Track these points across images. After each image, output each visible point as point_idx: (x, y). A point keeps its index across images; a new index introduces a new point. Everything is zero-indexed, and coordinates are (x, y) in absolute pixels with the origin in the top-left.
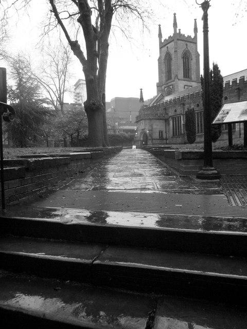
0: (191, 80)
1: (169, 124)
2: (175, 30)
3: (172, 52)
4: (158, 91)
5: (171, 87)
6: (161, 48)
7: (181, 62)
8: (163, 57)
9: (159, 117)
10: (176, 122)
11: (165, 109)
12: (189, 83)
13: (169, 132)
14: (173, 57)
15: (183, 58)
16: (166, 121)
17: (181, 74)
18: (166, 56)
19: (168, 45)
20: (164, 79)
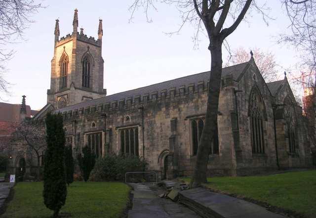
5: (66, 96)
12: (88, 94)
19: (65, 45)
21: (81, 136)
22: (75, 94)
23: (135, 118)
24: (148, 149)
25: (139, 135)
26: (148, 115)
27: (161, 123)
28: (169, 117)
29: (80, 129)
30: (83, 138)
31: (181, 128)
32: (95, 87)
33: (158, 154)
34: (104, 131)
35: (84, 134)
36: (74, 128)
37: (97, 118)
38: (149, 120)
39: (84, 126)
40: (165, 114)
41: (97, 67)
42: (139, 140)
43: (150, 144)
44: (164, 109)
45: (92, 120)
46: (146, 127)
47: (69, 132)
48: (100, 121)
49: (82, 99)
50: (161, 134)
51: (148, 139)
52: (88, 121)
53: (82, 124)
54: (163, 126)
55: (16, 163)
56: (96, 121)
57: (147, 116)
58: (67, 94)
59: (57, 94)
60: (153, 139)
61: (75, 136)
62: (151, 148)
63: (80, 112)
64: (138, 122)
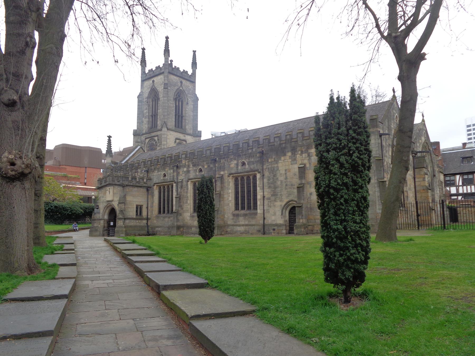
0: (185, 133)
1: (153, 196)
4: (135, 142)
9: (139, 182)
10: (164, 192)
11: (147, 172)
12: (181, 136)
13: (152, 207)
15: (175, 99)
16: (148, 190)
20: (145, 127)
21: (184, 183)
22: (167, 135)
23: (253, 164)
25: (258, 183)
26: (270, 161)
27: (286, 170)
28: (296, 163)
29: (183, 175)
30: (187, 185)
35: (188, 181)
36: (175, 174)
37: (205, 163)
38: (270, 166)
40: (290, 160)
42: (258, 188)
44: (289, 154)
45: (198, 165)
46: (267, 174)
47: (169, 179)
48: (209, 166)
49: (175, 142)
51: (269, 187)
53: (185, 169)
55: (104, 215)
57: (268, 161)
60: (275, 188)
61: (177, 183)
63: (184, 156)
64: (256, 168)
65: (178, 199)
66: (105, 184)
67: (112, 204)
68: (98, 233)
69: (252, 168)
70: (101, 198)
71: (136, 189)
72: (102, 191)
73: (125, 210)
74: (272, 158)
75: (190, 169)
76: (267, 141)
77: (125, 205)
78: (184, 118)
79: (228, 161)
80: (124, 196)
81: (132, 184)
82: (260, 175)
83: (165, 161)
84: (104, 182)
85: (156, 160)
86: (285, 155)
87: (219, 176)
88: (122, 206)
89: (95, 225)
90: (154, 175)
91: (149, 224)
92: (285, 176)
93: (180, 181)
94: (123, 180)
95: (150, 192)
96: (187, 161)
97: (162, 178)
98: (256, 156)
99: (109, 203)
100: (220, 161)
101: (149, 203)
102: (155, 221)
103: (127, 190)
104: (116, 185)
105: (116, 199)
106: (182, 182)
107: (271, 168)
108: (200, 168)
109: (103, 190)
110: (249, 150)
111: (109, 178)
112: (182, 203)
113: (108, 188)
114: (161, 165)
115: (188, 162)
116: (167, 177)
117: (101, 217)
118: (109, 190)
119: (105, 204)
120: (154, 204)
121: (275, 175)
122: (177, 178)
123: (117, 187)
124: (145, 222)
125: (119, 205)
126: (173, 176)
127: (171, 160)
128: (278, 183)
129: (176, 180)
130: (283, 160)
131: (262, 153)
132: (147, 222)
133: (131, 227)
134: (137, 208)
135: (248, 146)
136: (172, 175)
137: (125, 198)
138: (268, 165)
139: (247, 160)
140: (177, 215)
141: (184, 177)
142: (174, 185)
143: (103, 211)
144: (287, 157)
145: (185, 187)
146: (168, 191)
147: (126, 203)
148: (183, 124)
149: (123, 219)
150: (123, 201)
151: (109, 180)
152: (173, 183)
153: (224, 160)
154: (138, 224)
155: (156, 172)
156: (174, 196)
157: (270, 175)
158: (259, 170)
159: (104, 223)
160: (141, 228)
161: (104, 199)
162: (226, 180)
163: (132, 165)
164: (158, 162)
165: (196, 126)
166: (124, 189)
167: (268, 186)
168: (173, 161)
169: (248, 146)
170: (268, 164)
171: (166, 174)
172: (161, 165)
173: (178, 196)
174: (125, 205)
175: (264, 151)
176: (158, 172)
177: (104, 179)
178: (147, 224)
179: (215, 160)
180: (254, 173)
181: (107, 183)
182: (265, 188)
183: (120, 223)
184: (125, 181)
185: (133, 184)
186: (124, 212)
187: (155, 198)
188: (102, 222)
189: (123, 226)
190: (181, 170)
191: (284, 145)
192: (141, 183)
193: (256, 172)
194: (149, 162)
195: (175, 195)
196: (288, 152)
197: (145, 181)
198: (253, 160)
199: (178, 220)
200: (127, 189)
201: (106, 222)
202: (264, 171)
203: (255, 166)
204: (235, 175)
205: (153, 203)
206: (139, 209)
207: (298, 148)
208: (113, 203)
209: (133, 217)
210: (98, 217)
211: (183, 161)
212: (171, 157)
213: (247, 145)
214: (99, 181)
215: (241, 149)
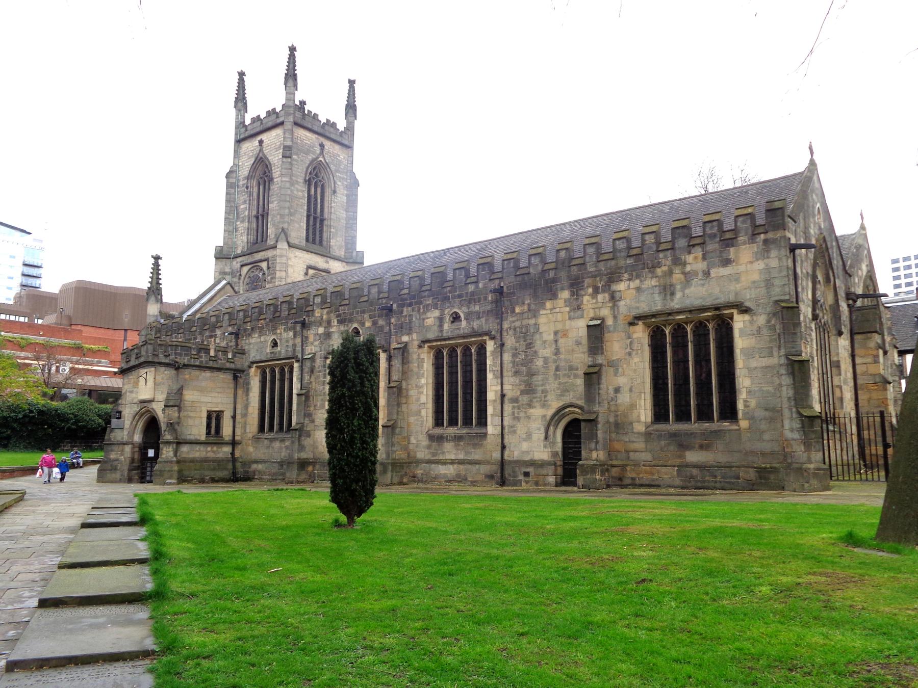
1: (247, 391)
2: (290, 95)
3: (275, 158)
5: (264, 265)
6: (239, 141)
7: (301, 192)
8: (245, 171)
9: (215, 359)
12: (320, 262)
13: (245, 415)
14: (276, 173)
16: (235, 378)
17: (298, 232)
18: (254, 168)
19: (264, 137)
22: (288, 259)
23: (479, 318)
24: (515, 400)
25: (489, 362)
26: (517, 310)
27: (556, 333)
28: (582, 317)
29: (317, 343)
31: (615, 346)
32: (336, 244)
33: (544, 416)
34: (385, 351)
36: (298, 340)
37: (366, 316)
38: (518, 324)
39: (328, 335)
40: (568, 309)
41: (341, 197)
42: (489, 376)
43: (522, 387)
44: (565, 294)
45: (351, 321)
46: (510, 341)
47: (283, 352)
48: (375, 323)
49: (306, 274)
50: (555, 361)
51: (516, 373)
52: (339, 322)
53: (321, 330)
54: (562, 341)
55: (131, 434)
56: (363, 324)
57: (513, 311)
58: (267, 260)
59: (239, 259)
60: (531, 374)
61: (302, 361)
62: (525, 399)
63: (318, 300)
64: (485, 328)
65: (303, 398)
66: (137, 363)
67: (153, 409)
68: (118, 475)
69: (475, 327)
70: (128, 394)
71: (208, 374)
72: (131, 377)
73: (178, 423)
74: (523, 304)
75: (331, 330)
76: (512, 265)
77: (179, 411)
78: (326, 223)
79: (419, 309)
80: (179, 390)
81: (197, 363)
82: (495, 344)
83: (275, 311)
84: (134, 356)
85: (257, 310)
86: (554, 296)
87: (399, 346)
88: (174, 413)
89: (113, 456)
90: (250, 344)
91: (237, 454)
92: (554, 346)
93: (310, 356)
94: (176, 354)
95: (241, 381)
96: (325, 311)
97: (268, 351)
98: (486, 298)
99: (146, 405)
100: (402, 312)
101: (239, 406)
102: (251, 449)
103: (187, 376)
104: (160, 364)
105: (161, 397)
106: (313, 359)
107: (521, 328)
108: (355, 328)
109: (132, 376)
110: (470, 286)
111: (147, 348)
112: (312, 409)
113: (142, 371)
114: (268, 320)
115: (328, 313)
116: (279, 348)
117: (126, 439)
118: (144, 376)
119: (136, 408)
120: (250, 409)
121: (530, 344)
122: (303, 350)
123: (162, 369)
124: (227, 449)
125: (167, 411)
126: (294, 345)
127: (290, 310)
128: (537, 363)
129: (300, 356)
130: (551, 309)
131: (500, 291)
132: (233, 450)
133: (193, 461)
134: (209, 417)
135: (467, 276)
136: (291, 343)
137: (181, 394)
138: (514, 322)
139: (465, 309)
140: (300, 436)
141: (318, 349)
142: (296, 365)
143: (131, 423)
144: (560, 303)
145: (320, 371)
146: (282, 381)
147: (182, 405)
148: (325, 235)
149: (174, 443)
150: (175, 401)
151: (147, 352)
152: (294, 360)
153: (410, 309)
154: (211, 455)
155: (256, 336)
156: (295, 392)
157: (518, 345)
158: (493, 333)
159: (133, 453)
160: (219, 463)
161: (134, 395)
162: (415, 356)
163: (204, 321)
164: (261, 313)
165: (351, 242)
166: (178, 375)
167: (513, 370)
168: (294, 311)
169: (467, 276)
170: (514, 319)
171: (278, 341)
172: (268, 320)
173: (304, 391)
174: (179, 411)
175: (505, 288)
176: (260, 336)
177: (136, 351)
178: (233, 454)
179: (390, 309)
180: (480, 338)
181: (142, 360)
182: (505, 374)
183: (167, 452)
184: (180, 354)
185: (201, 362)
186: (176, 426)
187: (251, 395)
188: (128, 449)
189: (175, 459)
190: (312, 332)
191: (552, 274)
192: (219, 361)
193: (484, 338)
194: (241, 314)
195: (297, 389)
196: (562, 289)
197: (230, 356)
198: (477, 308)
199: (302, 448)
200: (187, 374)
201: (137, 449)
202: (505, 334)
203: (484, 322)
204: (434, 344)
205: (246, 407)
206: (214, 419)
207: (587, 281)
208: (154, 405)
209: (198, 438)
210: (119, 438)
211: (317, 311)
212: (290, 303)
213: (463, 273)
214: (124, 356)
215: (451, 284)
